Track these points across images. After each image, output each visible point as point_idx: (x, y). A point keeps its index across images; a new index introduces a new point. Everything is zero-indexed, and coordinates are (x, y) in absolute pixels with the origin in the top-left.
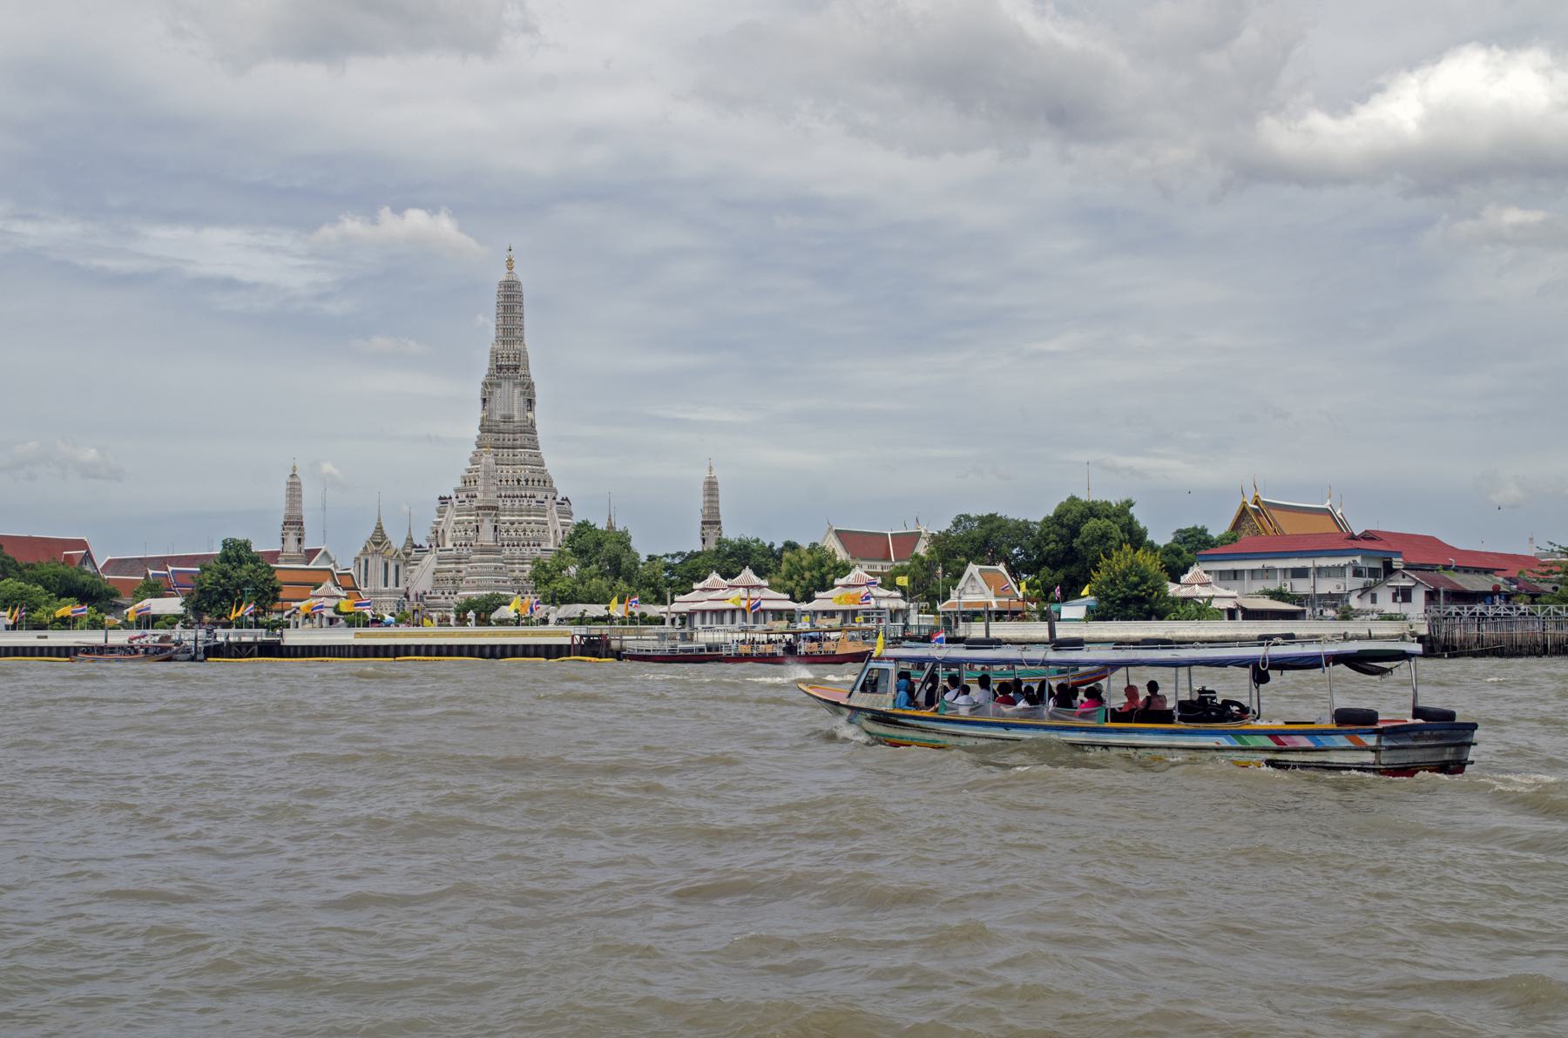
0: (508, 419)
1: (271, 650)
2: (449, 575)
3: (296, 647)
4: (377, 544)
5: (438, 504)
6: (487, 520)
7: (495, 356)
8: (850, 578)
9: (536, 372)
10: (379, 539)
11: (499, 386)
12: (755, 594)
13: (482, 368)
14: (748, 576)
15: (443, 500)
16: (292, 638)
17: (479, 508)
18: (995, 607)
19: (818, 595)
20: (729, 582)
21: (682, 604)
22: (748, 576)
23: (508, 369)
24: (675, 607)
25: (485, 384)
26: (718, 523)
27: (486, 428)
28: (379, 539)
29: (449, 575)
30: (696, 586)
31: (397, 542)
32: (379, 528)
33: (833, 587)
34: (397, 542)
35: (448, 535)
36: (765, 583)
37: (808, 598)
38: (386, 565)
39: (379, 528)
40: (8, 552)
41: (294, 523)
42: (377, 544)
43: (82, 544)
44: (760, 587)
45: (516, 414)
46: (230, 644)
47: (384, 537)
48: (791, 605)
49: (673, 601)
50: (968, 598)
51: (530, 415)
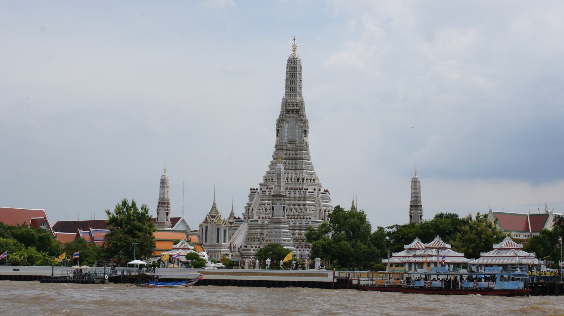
0: (291, 142)
2: (255, 236)
5: (249, 192)
6: (278, 203)
7: (285, 103)
8: (503, 244)
9: (309, 112)
10: (214, 214)
11: (287, 122)
12: (443, 253)
13: (277, 110)
14: (437, 241)
15: (253, 191)
16: (161, 273)
17: (274, 196)
19: (482, 254)
20: (426, 245)
21: (397, 258)
22: (437, 241)
23: (292, 112)
24: (392, 260)
25: (278, 120)
27: (279, 147)
28: (214, 214)
29: (255, 236)
30: (406, 247)
31: (225, 215)
32: (214, 207)
33: (493, 249)
34: (225, 215)
35: (255, 211)
36: (449, 246)
37: (477, 257)
38: (218, 229)
39: (214, 207)
41: (163, 203)
44: (445, 248)
45: (297, 138)
46: (124, 276)
47: (217, 212)
48: (465, 260)
49: (391, 256)
51: (305, 139)
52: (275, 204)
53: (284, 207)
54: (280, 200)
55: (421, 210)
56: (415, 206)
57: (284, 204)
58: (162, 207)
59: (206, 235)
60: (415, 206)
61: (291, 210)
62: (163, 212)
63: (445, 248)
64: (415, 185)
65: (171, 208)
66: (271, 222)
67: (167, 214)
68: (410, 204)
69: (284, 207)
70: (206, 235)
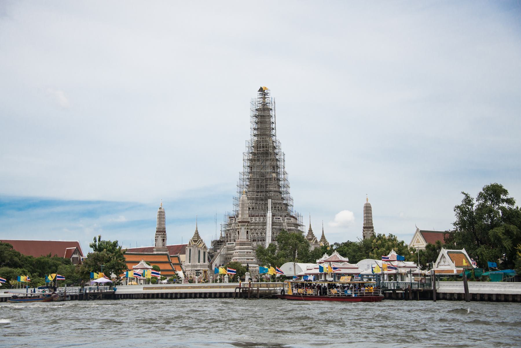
1: (113, 296)
3: (121, 295)
4: (195, 241)
6: (243, 228)
7: (257, 146)
17: (239, 222)
18: (455, 272)
26: (373, 227)
32: (197, 233)
36: (347, 259)
38: (199, 251)
39: (197, 233)
40: (15, 249)
42: (195, 241)
43: (76, 244)
44: (341, 262)
46: (86, 293)
47: (198, 237)
50: (441, 268)
52: (241, 229)
53: (247, 232)
54: (244, 225)
55: (372, 231)
56: (368, 227)
57: (248, 229)
58: (159, 235)
59: (190, 256)
60: (368, 227)
61: (257, 233)
62: (160, 239)
63: (341, 262)
64: (368, 209)
65: (167, 235)
66: (237, 244)
67: (163, 240)
68: (363, 226)
69: (247, 232)
70: (190, 256)
